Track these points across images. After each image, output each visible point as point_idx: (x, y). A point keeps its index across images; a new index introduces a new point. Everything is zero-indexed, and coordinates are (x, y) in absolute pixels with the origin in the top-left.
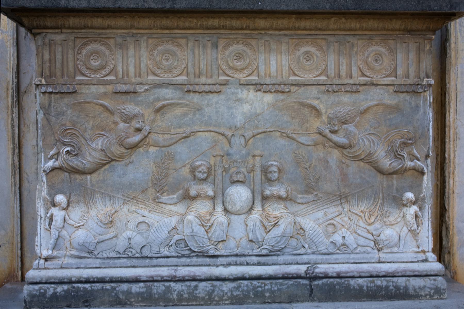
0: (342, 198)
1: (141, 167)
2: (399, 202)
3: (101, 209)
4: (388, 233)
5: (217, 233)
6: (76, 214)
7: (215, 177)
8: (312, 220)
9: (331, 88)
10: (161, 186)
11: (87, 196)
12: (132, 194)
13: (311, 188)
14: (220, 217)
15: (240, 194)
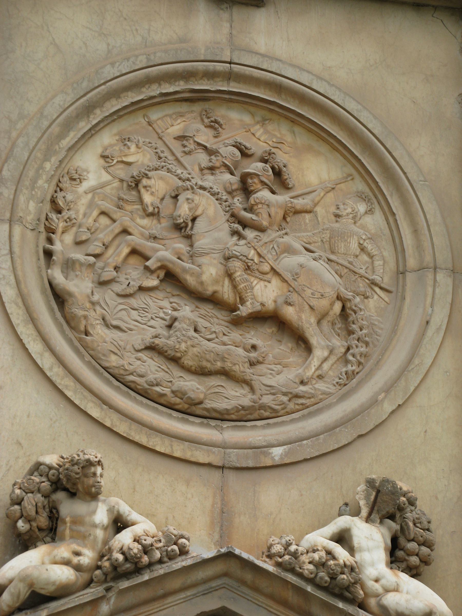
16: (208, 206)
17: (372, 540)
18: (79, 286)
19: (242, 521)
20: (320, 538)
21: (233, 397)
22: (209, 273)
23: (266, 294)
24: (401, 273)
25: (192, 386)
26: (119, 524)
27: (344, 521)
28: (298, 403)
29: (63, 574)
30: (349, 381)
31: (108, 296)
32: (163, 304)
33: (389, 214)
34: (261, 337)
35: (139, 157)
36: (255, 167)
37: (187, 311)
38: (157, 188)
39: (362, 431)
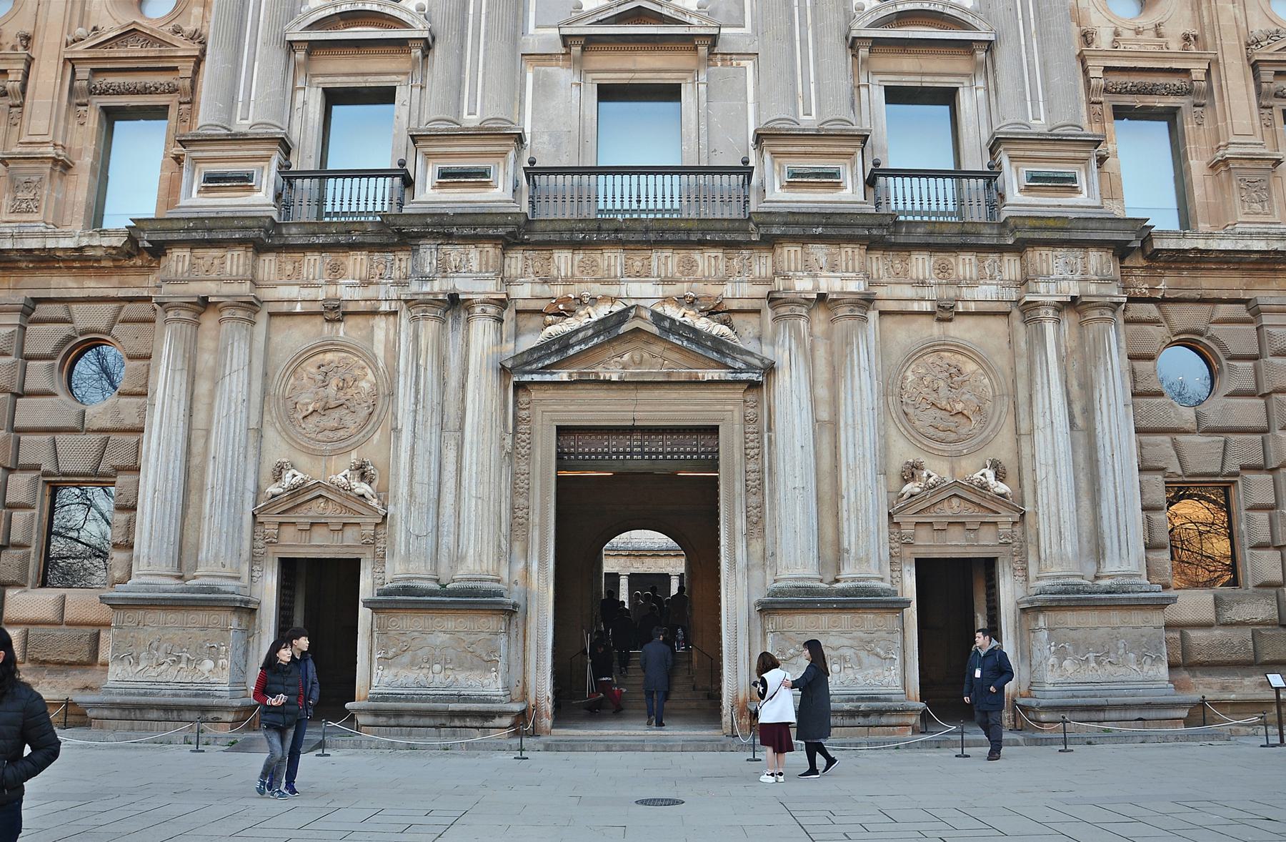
0: (471, 669)
1: (406, 658)
2: (490, 671)
3: (394, 671)
4: (486, 682)
5: (430, 680)
6: (386, 672)
7: (431, 661)
8: (461, 676)
9: (469, 633)
10: (412, 664)
11: (389, 666)
12: (403, 667)
13: (461, 666)
14: (431, 675)
15: (437, 667)
16: (942, 384)
17: (990, 474)
18: (910, 411)
19: (957, 470)
20: (977, 475)
21: (952, 436)
22: (944, 404)
23: (959, 407)
24: (994, 396)
25: (941, 434)
26: (929, 476)
27: (983, 471)
28: (970, 436)
29: (918, 490)
30: (983, 429)
31: (918, 412)
32: (933, 412)
33: (990, 379)
34: (959, 418)
35: (922, 371)
36: (953, 370)
37: (939, 414)
38: (928, 378)
39: (986, 443)
